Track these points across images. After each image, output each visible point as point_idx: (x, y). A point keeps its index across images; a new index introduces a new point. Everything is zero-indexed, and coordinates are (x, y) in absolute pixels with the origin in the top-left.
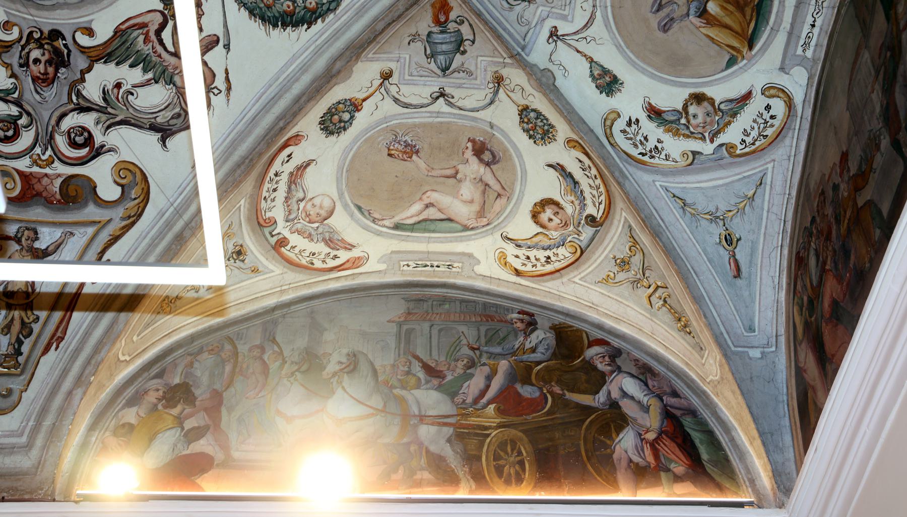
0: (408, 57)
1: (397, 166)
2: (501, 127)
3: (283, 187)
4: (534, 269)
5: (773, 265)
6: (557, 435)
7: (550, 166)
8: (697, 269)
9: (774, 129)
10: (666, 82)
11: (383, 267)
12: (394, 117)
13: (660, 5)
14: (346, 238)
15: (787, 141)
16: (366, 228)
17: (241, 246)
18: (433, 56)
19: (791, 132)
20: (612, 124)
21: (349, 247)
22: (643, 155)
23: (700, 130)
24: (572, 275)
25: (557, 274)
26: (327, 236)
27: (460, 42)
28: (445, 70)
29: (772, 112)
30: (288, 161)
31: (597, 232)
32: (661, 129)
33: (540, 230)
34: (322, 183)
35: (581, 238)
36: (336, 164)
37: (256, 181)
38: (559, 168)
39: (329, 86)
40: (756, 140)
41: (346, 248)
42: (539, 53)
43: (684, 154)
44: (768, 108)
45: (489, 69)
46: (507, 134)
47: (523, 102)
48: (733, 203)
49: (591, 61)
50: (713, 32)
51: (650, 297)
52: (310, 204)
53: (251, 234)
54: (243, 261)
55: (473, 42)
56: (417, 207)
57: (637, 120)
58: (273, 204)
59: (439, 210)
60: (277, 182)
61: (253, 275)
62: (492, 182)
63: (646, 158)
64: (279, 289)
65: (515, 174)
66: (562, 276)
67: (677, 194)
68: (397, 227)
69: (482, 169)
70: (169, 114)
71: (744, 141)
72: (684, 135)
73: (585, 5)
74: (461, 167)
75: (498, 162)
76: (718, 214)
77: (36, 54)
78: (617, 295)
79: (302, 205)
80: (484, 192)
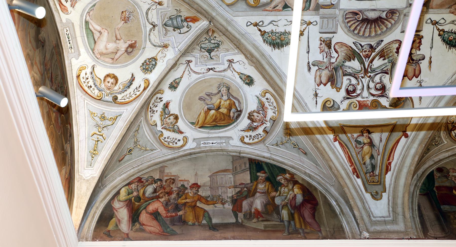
1: (118, 16)
4: (83, 83)
7: (133, 75)
11: (64, 21)
12: (141, 10)
13: (209, 95)
14: (77, 4)
15: (170, 151)
16: (84, 10)
18: (171, 19)
22: (151, 108)
23: (165, 123)
24: (87, 99)
25: (85, 93)
27: (179, 28)
28: (165, 25)
29: (178, 142)
31: (111, 102)
32: (161, 110)
33: (102, 80)
35: (106, 97)
41: (72, 4)
42: (183, 60)
44: (179, 140)
47: (158, 58)
49: (181, 78)
50: (203, 114)
55: (180, 33)
56: (99, 28)
57: (162, 101)
59: (99, 37)
62: (118, 55)
63: (149, 110)
65: (124, 63)
66: (85, 95)
68: (87, 23)
69: (123, 49)
73: (203, 70)
74: (122, 41)
78: (88, 120)
80: (112, 53)
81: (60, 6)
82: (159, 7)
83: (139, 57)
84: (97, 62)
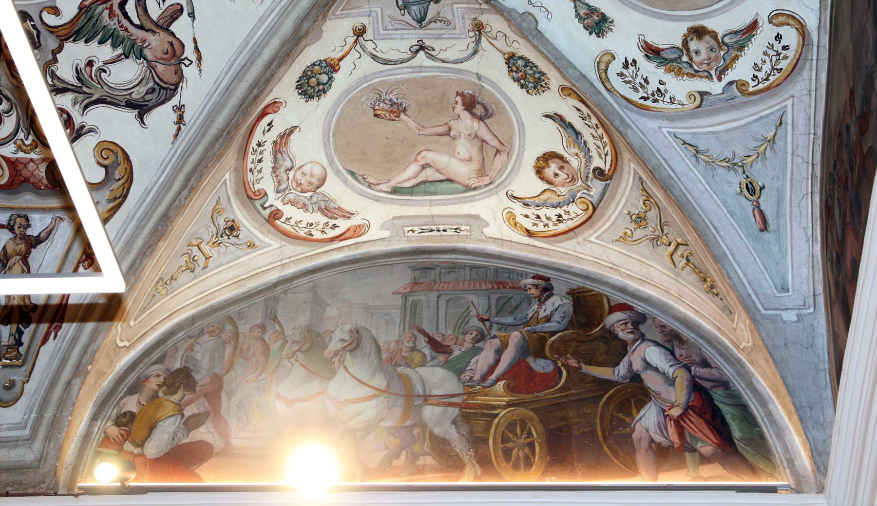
0: (379, 10)
1: (386, 127)
2: (489, 77)
3: (268, 157)
5: (804, 215)
6: (571, 414)
7: (547, 116)
8: (715, 223)
9: (788, 61)
10: (660, 17)
11: (386, 234)
12: (375, 75)
14: (342, 206)
15: (805, 74)
16: (362, 194)
17: (233, 221)
19: (808, 63)
20: (607, 67)
21: (348, 215)
23: (705, 67)
24: (587, 234)
25: (572, 234)
26: (322, 204)
28: (420, 20)
29: (784, 42)
30: (269, 130)
31: (607, 186)
32: (662, 70)
33: (547, 186)
34: (309, 150)
35: (592, 193)
36: (321, 130)
37: (238, 153)
38: (558, 118)
39: (299, 48)
40: (769, 75)
41: (344, 216)
43: (690, 95)
44: (778, 37)
45: (466, 17)
46: (495, 84)
48: (751, 147)
51: (672, 255)
52: (299, 172)
53: (242, 209)
54: (237, 236)
56: (413, 169)
57: (634, 61)
58: (260, 175)
59: (437, 171)
60: (261, 153)
61: (249, 250)
62: (488, 137)
63: (649, 103)
64: (279, 263)
65: (511, 127)
66: (576, 236)
67: (688, 140)
68: (395, 191)
69: (476, 124)
70: (143, 89)
71: (756, 77)
72: (688, 74)
74: (453, 124)
75: (491, 115)
76: (736, 161)
78: (637, 254)
79: (291, 174)
80: (481, 149)
81: (345, 239)
82: (368, 35)
83: (502, 92)
84: (501, 187)
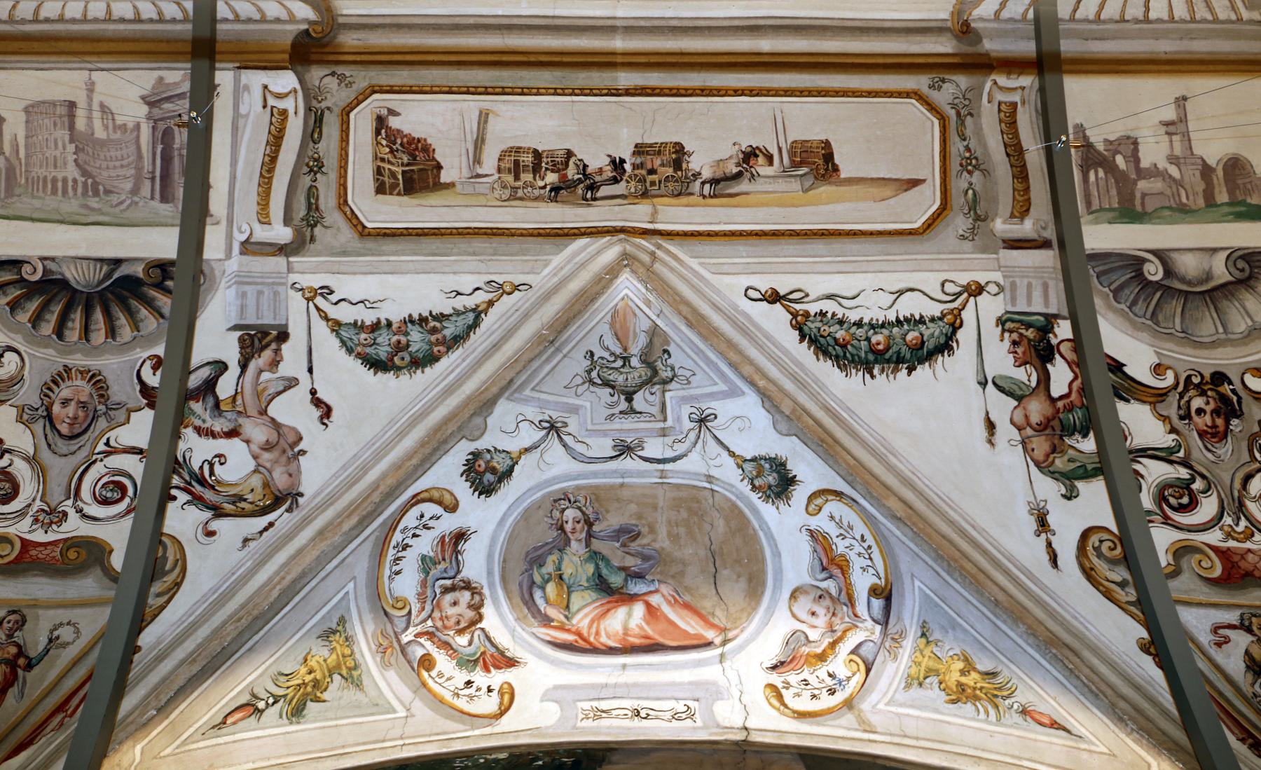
77: (1197, 403)
